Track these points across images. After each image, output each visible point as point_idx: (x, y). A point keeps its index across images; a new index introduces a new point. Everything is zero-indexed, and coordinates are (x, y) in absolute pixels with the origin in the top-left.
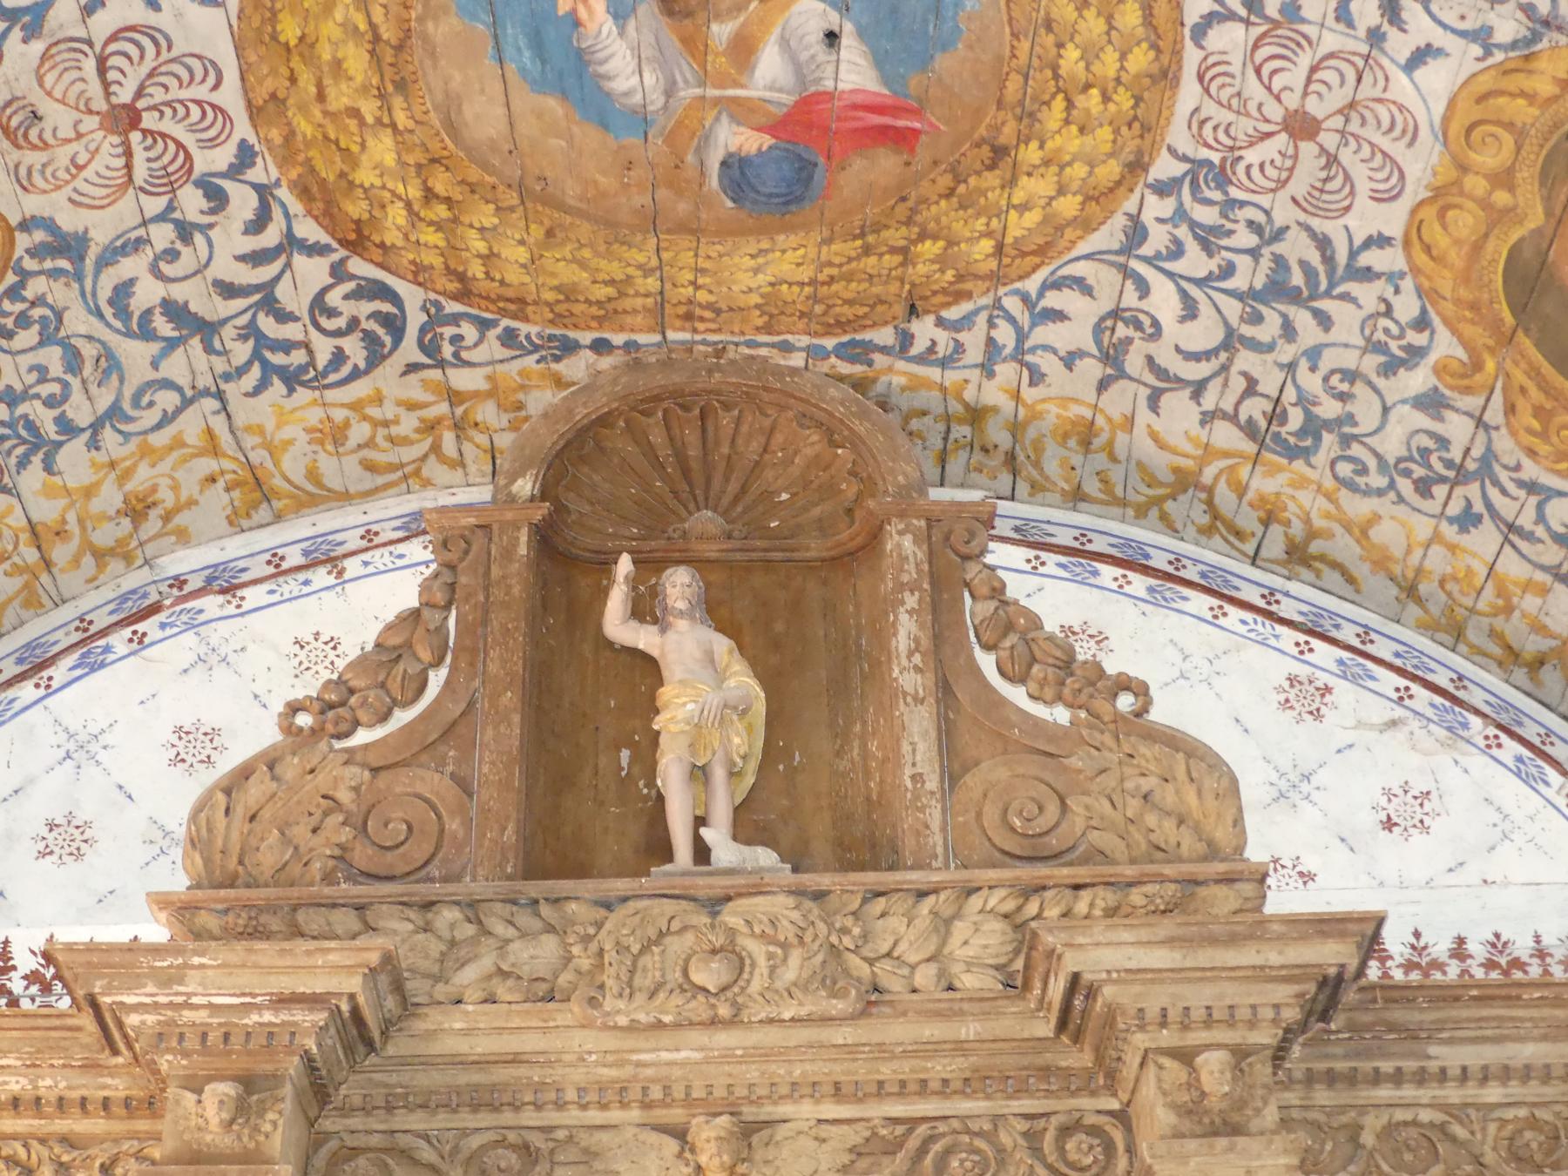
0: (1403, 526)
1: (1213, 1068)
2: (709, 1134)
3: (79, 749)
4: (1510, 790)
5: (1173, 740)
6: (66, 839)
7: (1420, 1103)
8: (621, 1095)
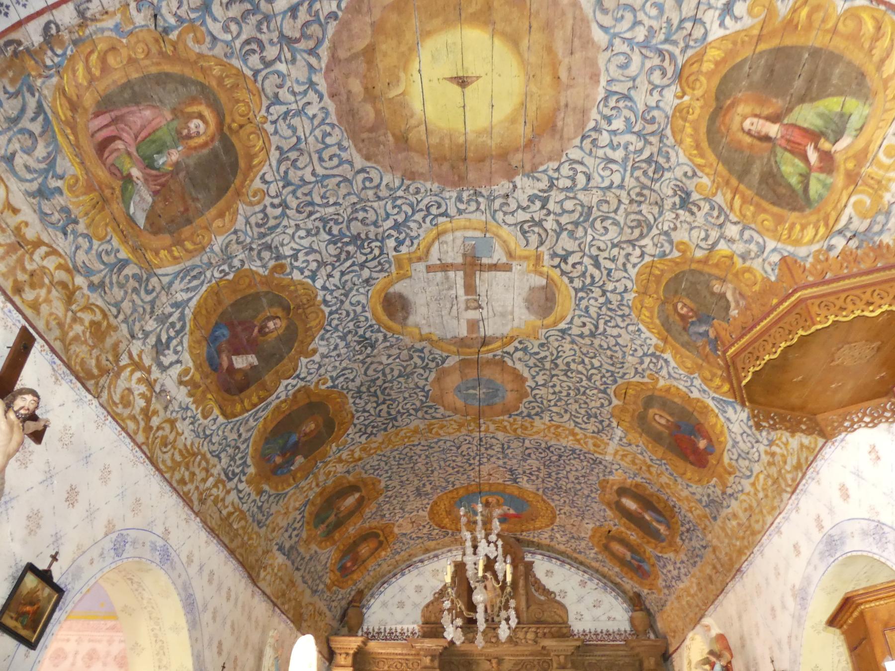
0: (594, 564)
1: (562, 658)
2: (494, 661)
3: (402, 589)
4: (613, 600)
5: (559, 603)
6: (401, 605)
7: (593, 660)
8: (482, 655)
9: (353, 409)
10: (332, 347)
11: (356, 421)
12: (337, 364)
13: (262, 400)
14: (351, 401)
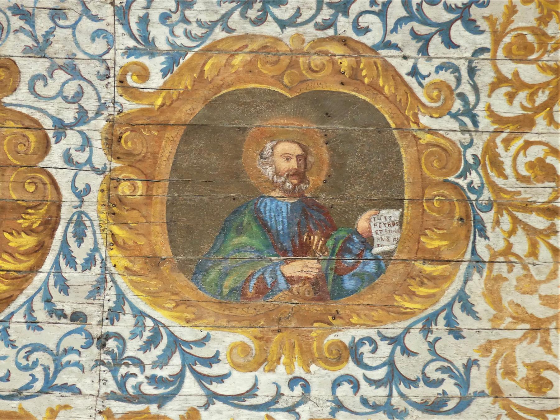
9: (310, 32)
10: (17, 22)
11: (372, 38)
12: (87, 25)
13: (50, 225)
14: (270, 29)
